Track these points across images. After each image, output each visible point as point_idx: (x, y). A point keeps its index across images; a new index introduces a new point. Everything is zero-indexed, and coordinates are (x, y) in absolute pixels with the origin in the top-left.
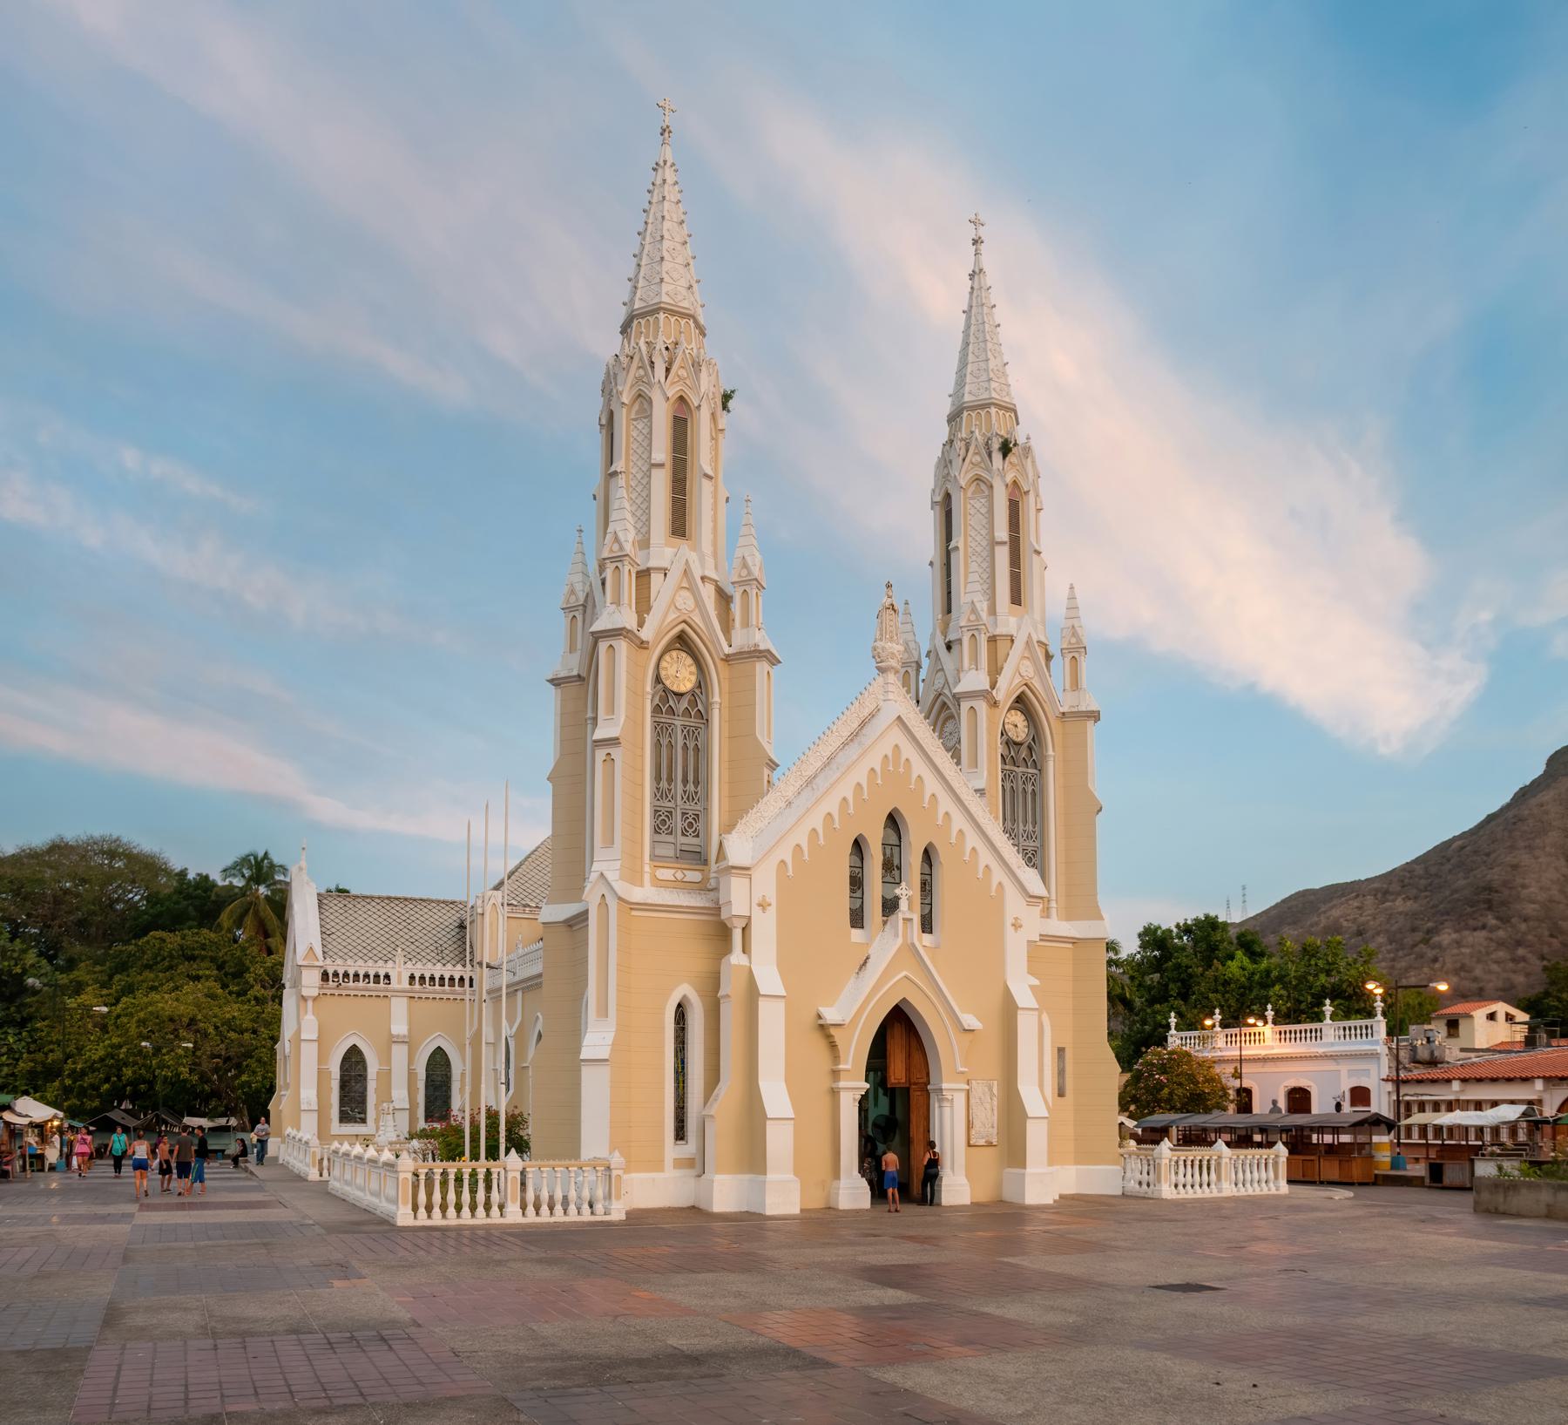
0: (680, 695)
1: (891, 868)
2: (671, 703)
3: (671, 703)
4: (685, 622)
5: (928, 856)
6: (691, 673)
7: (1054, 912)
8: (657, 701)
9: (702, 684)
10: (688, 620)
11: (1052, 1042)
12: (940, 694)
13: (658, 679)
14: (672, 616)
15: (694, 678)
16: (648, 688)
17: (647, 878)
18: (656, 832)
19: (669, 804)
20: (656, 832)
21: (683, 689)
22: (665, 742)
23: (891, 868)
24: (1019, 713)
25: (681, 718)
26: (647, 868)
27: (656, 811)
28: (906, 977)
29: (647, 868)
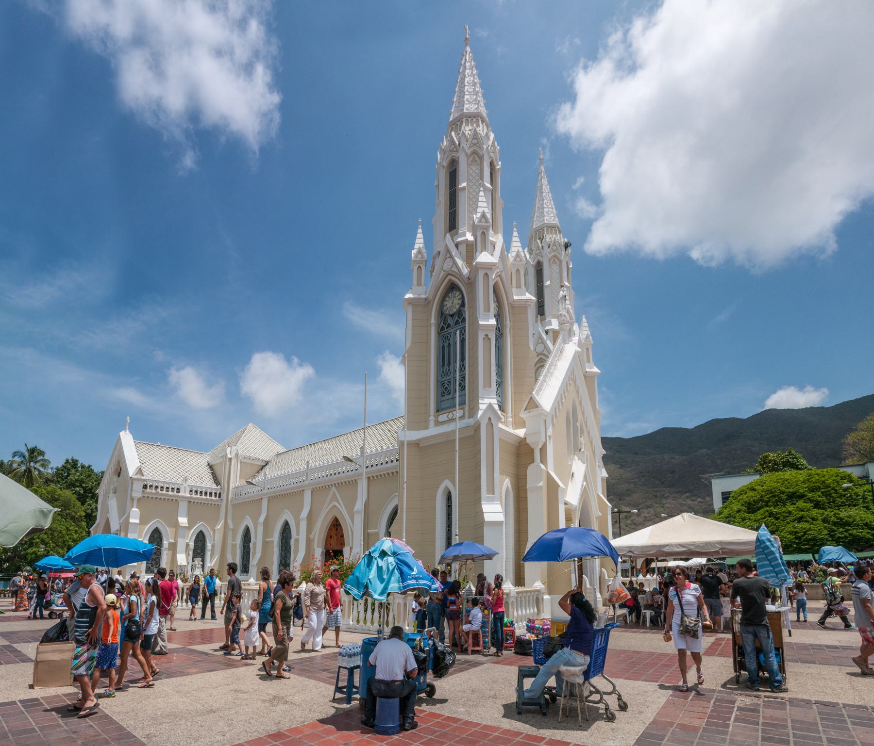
0: (452, 316)
2: (449, 322)
3: (449, 322)
4: (449, 274)
6: (459, 299)
13: (442, 314)
14: (441, 275)
15: (460, 302)
17: (432, 423)
18: (442, 396)
19: (448, 378)
20: (442, 396)
21: (455, 310)
22: (446, 344)
26: (432, 418)
27: (442, 384)
29: (432, 418)
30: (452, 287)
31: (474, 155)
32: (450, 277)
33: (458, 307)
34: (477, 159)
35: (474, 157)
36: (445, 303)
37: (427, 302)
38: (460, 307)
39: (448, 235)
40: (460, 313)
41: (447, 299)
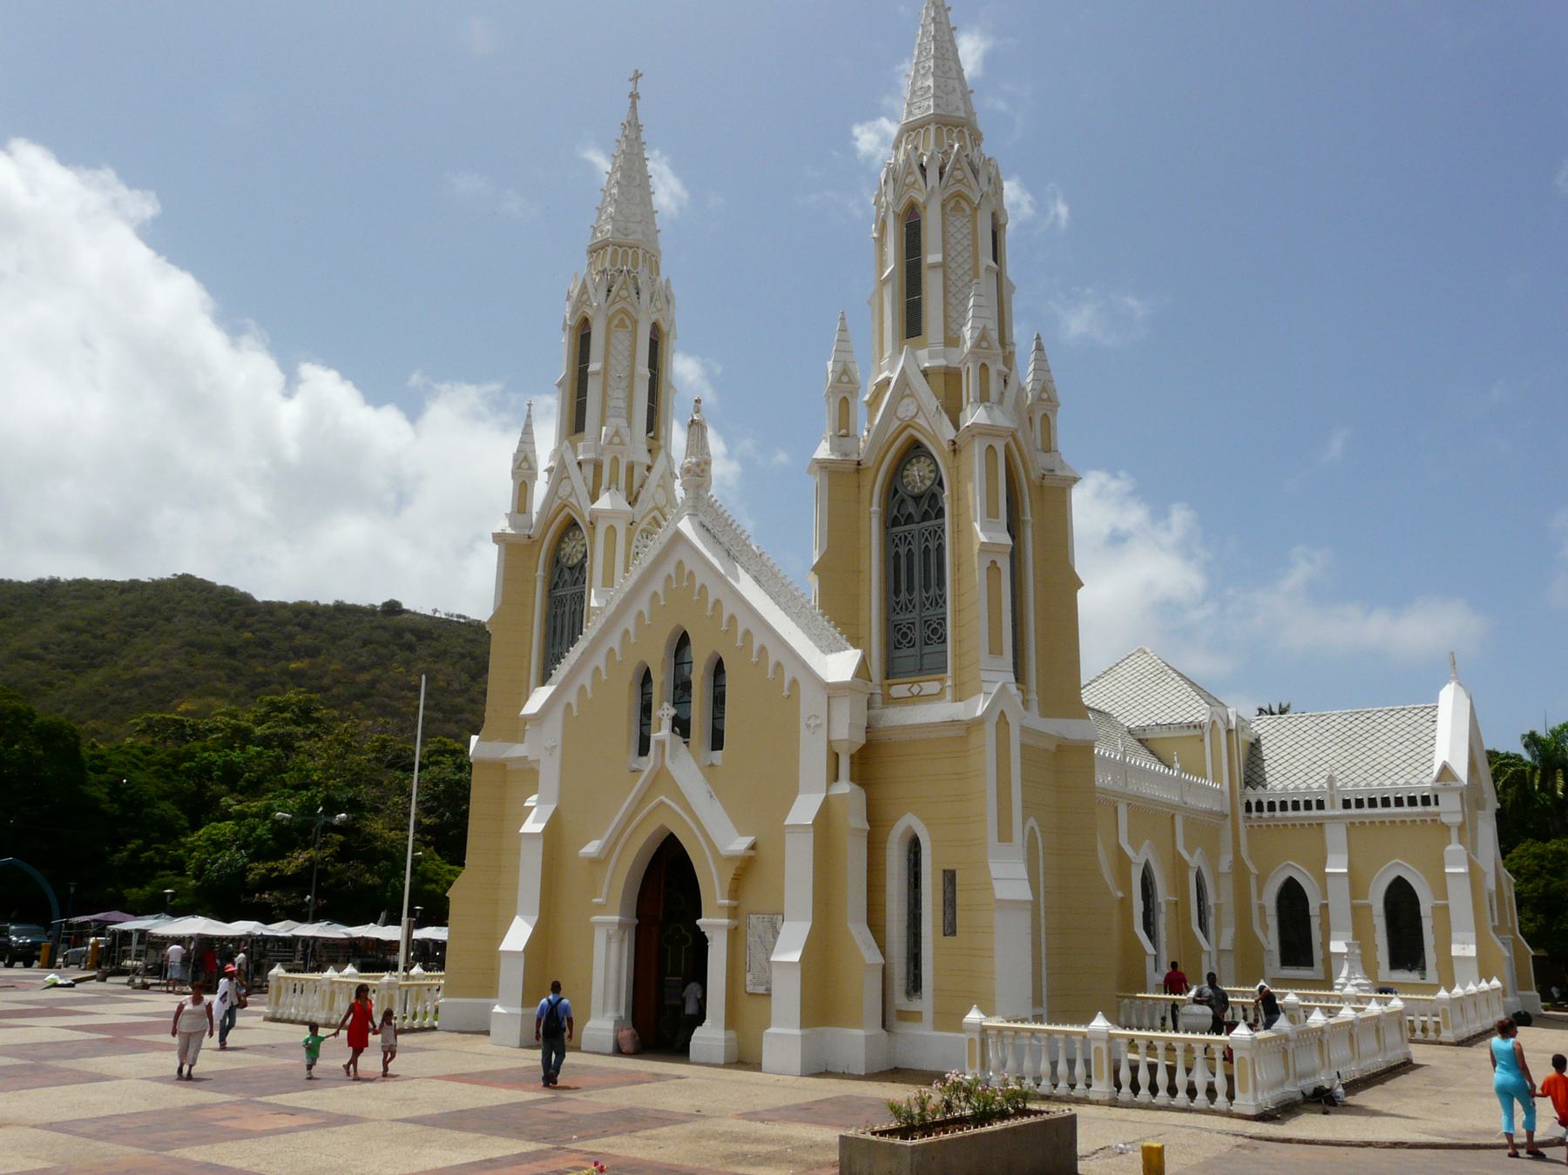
0: (571, 569)
1: (682, 689)
5: (718, 669)
7: (949, 694)
8: (556, 579)
9: (585, 556)
10: (566, 502)
11: (934, 863)
12: (566, 506)
13: (558, 561)
16: (540, 573)
21: (576, 561)
23: (682, 689)
24: (923, 459)
25: (573, 587)
28: (662, 803)
30: (572, 525)
31: (623, 315)
32: (567, 508)
33: (580, 556)
34: (627, 322)
35: (622, 320)
36: (564, 545)
37: (531, 542)
38: (583, 558)
39: (566, 443)
40: (581, 566)
41: (566, 539)
